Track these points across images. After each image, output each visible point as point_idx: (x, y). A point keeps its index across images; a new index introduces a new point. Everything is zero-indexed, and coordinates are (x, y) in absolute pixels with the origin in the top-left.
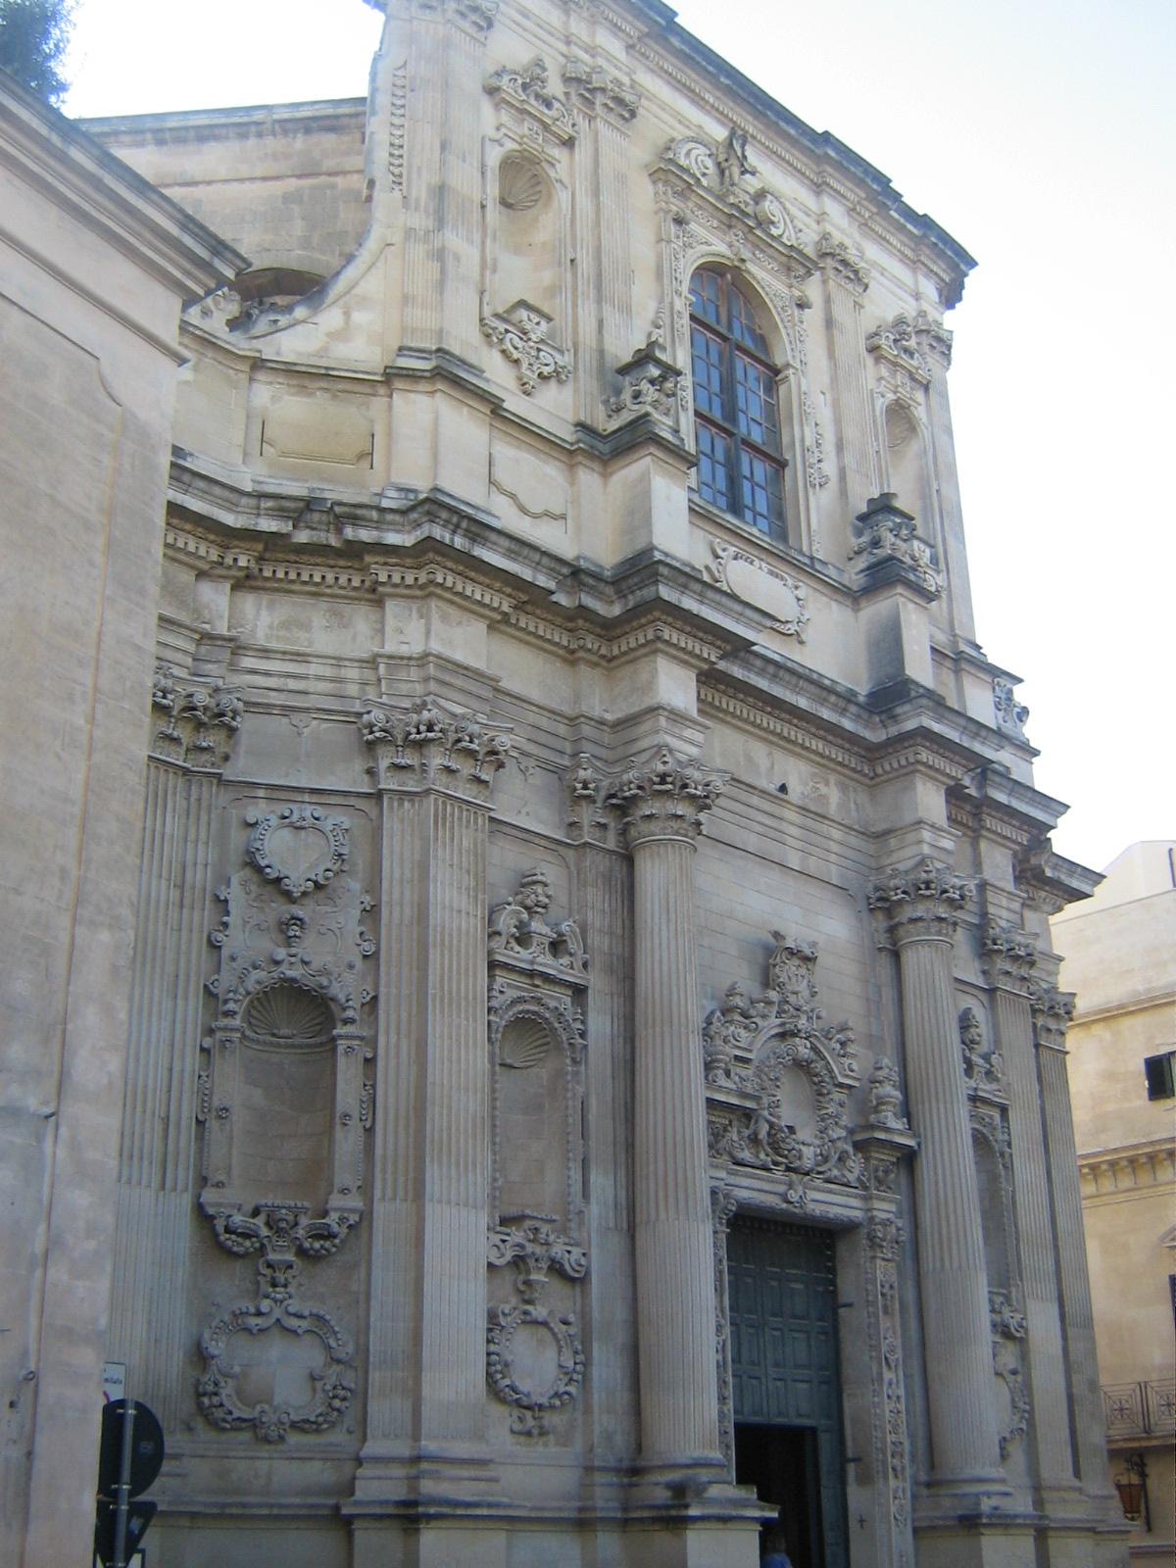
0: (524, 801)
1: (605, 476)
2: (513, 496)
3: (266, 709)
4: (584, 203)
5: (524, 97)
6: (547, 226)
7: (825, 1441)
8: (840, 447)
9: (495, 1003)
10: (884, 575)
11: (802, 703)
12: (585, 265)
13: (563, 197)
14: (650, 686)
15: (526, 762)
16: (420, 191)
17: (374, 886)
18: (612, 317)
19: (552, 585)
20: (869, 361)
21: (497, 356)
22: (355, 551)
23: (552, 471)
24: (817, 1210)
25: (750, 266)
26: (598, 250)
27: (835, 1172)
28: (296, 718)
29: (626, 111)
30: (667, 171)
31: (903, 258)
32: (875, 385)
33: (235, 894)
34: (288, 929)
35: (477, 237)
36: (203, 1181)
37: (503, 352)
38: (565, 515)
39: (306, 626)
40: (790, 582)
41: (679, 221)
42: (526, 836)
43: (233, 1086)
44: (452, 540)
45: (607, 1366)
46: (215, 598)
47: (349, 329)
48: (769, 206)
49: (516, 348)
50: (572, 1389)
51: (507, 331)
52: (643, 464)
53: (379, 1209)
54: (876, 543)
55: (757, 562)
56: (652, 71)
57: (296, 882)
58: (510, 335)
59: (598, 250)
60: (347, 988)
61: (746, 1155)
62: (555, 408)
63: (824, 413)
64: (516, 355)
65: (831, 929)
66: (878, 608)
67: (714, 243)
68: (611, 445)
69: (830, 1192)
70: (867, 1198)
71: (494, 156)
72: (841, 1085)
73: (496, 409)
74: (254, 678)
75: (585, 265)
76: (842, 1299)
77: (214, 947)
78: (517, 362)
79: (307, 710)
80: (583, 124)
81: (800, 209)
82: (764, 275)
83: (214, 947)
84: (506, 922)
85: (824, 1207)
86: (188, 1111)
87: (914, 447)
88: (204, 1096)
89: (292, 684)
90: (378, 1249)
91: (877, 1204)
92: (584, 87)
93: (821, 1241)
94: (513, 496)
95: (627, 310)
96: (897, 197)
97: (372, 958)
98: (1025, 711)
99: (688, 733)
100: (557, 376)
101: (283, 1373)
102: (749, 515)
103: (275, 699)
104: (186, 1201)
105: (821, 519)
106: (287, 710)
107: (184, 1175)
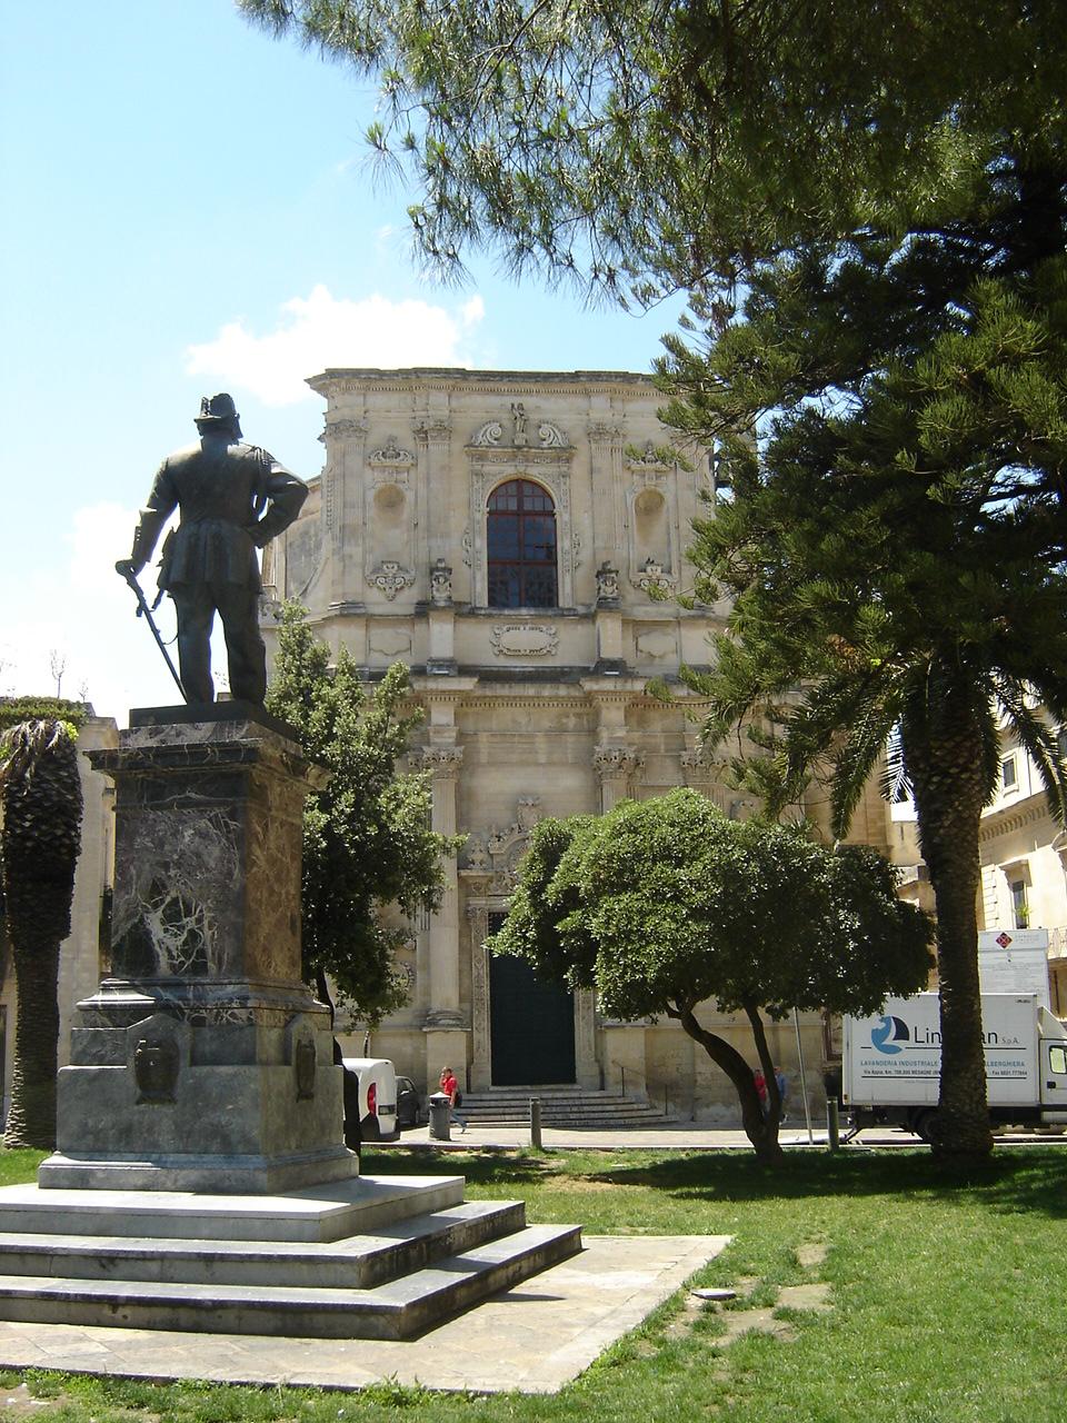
2: (381, 651)
4: (422, 491)
6: (407, 512)
13: (409, 496)
20: (627, 475)
23: (404, 630)
26: (429, 511)
35: (360, 542)
48: (545, 431)
59: (429, 511)
61: (499, 892)
62: (407, 600)
63: (583, 520)
68: (424, 610)
71: (371, 495)
82: (538, 473)
94: (381, 651)
105: (571, 586)
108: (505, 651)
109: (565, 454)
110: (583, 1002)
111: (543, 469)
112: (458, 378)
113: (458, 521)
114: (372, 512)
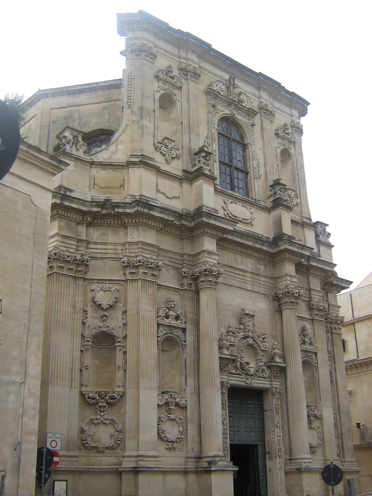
0: (168, 278)
1: (191, 184)
2: (164, 194)
3: (96, 258)
4: (185, 105)
5: (166, 77)
6: (175, 113)
7: (260, 449)
8: (265, 166)
9: (159, 335)
10: (277, 203)
11: (250, 244)
12: (185, 123)
13: (178, 105)
14: (202, 245)
15: (168, 267)
16: (136, 109)
17: (125, 305)
18: (193, 138)
19: (173, 219)
20: (275, 138)
21: (159, 154)
22: (119, 215)
23: (175, 185)
24: (256, 385)
25: (236, 116)
26: (189, 118)
27: (261, 374)
28: (104, 260)
29: (196, 76)
30: (210, 93)
31: (287, 105)
32: (276, 145)
33: (89, 309)
34: (104, 318)
35: (152, 120)
36: (82, 385)
37: (161, 152)
38: (176, 198)
39: (107, 235)
40: (248, 207)
41: (214, 106)
42: (168, 288)
43: (89, 359)
44: (144, 210)
45: (192, 430)
46: (82, 230)
47: (116, 151)
48: (243, 97)
49: (164, 151)
50: (182, 436)
51: (162, 146)
52: (200, 182)
53: (128, 391)
54: (275, 194)
55: (238, 203)
56: (207, 62)
57: (105, 305)
58: (162, 147)
59: (189, 118)
60: (119, 333)
61: (234, 371)
62: (176, 168)
63: (260, 156)
64: (164, 153)
65: (260, 306)
66: (275, 213)
67: (226, 111)
68: (191, 176)
69: (260, 380)
70: (271, 381)
71: (158, 96)
72: (263, 350)
73: (158, 170)
74: (95, 250)
75: (185, 123)
76: (265, 409)
77: (84, 324)
78: (165, 155)
79: (107, 258)
80: (184, 81)
81: (251, 96)
82: (241, 118)
83: (84, 324)
84: (162, 313)
85: (258, 385)
86: (77, 367)
87: (290, 162)
88: (82, 363)
89: (103, 251)
90: (128, 402)
91: (274, 383)
92: (185, 72)
93: (258, 395)
94: (164, 194)
95: (198, 135)
96: (283, 88)
97: (125, 325)
98: (329, 234)
99: (213, 257)
100: (177, 157)
101: (104, 435)
102: (236, 189)
103: (99, 255)
104: (76, 392)
105: (259, 189)
106: (102, 258)
107: (77, 384)
108: (230, 215)
109: (251, 113)
110: (278, 452)
111: (242, 118)
112: (206, 51)
113: (203, 131)
114: (157, 105)
